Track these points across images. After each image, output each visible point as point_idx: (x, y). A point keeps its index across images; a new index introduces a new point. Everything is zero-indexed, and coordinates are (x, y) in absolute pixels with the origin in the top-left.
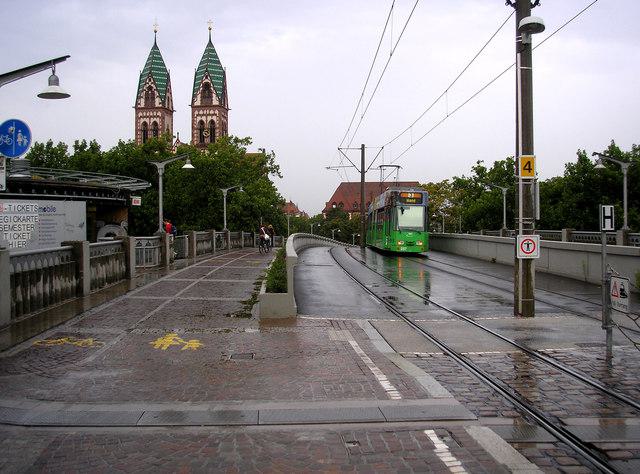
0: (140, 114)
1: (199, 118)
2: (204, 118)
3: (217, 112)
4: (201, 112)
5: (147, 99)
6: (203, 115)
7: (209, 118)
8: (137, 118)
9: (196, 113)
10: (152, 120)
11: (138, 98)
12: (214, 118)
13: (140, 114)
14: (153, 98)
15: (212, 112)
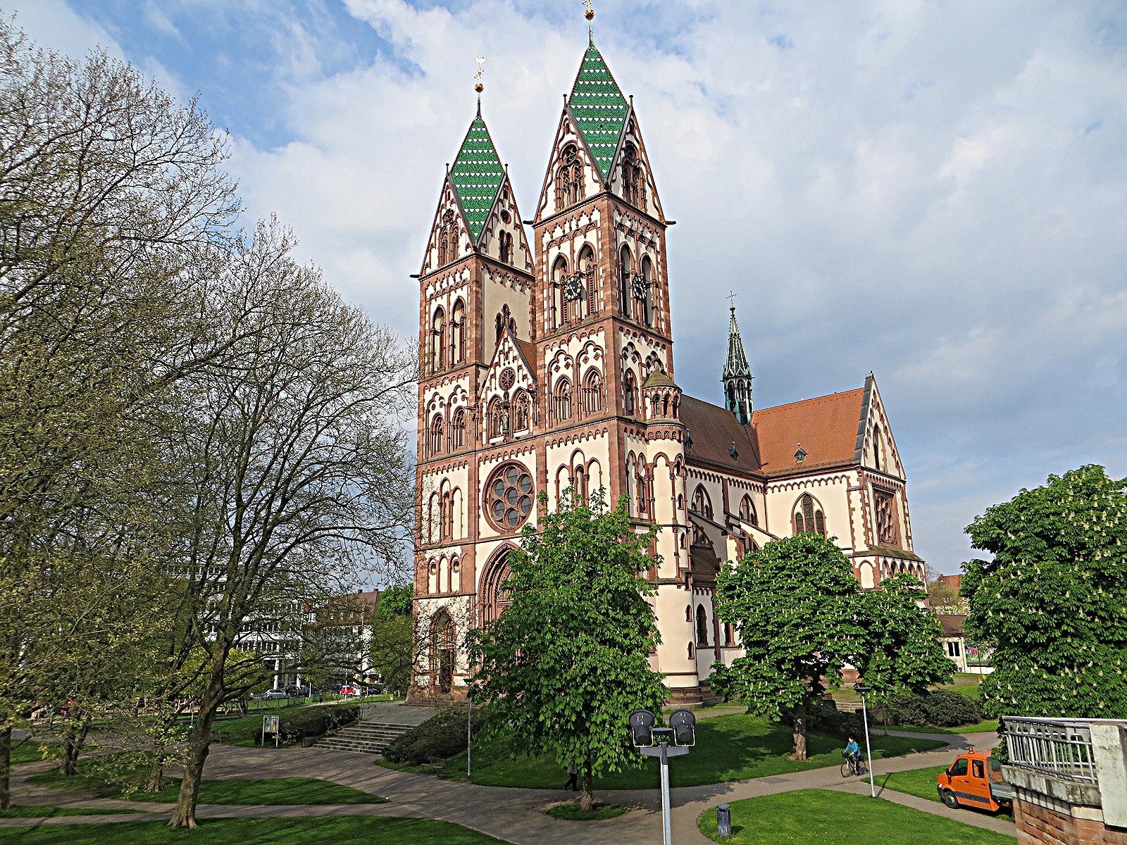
0: (430, 291)
1: (554, 252)
2: (565, 248)
3: (596, 216)
4: (558, 233)
5: (443, 247)
6: (561, 240)
7: (579, 242)
8: (426, 301)
9: (547, 238)
10: (454, 297)
11: (430, 248)
12: (592, 237)
13: (430, 291)
14: (455, 241)
15: (584, 221)
